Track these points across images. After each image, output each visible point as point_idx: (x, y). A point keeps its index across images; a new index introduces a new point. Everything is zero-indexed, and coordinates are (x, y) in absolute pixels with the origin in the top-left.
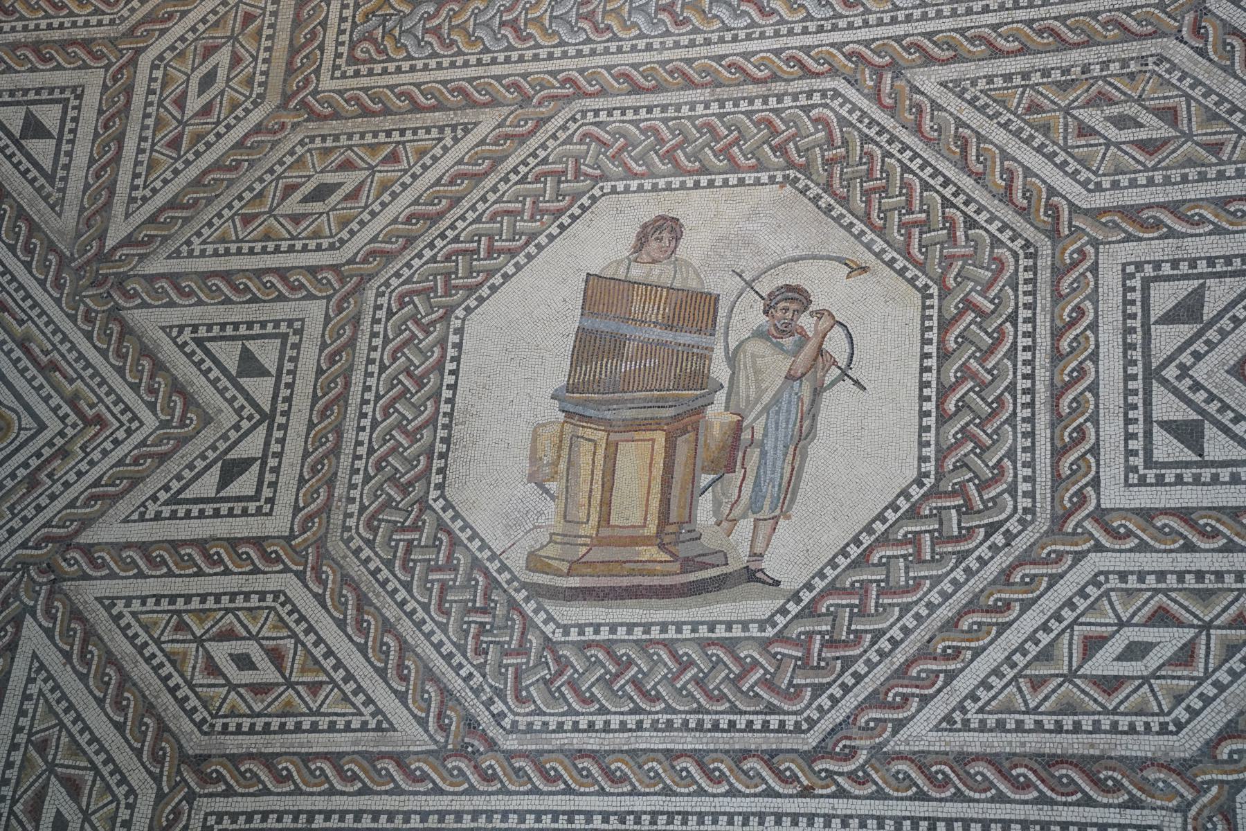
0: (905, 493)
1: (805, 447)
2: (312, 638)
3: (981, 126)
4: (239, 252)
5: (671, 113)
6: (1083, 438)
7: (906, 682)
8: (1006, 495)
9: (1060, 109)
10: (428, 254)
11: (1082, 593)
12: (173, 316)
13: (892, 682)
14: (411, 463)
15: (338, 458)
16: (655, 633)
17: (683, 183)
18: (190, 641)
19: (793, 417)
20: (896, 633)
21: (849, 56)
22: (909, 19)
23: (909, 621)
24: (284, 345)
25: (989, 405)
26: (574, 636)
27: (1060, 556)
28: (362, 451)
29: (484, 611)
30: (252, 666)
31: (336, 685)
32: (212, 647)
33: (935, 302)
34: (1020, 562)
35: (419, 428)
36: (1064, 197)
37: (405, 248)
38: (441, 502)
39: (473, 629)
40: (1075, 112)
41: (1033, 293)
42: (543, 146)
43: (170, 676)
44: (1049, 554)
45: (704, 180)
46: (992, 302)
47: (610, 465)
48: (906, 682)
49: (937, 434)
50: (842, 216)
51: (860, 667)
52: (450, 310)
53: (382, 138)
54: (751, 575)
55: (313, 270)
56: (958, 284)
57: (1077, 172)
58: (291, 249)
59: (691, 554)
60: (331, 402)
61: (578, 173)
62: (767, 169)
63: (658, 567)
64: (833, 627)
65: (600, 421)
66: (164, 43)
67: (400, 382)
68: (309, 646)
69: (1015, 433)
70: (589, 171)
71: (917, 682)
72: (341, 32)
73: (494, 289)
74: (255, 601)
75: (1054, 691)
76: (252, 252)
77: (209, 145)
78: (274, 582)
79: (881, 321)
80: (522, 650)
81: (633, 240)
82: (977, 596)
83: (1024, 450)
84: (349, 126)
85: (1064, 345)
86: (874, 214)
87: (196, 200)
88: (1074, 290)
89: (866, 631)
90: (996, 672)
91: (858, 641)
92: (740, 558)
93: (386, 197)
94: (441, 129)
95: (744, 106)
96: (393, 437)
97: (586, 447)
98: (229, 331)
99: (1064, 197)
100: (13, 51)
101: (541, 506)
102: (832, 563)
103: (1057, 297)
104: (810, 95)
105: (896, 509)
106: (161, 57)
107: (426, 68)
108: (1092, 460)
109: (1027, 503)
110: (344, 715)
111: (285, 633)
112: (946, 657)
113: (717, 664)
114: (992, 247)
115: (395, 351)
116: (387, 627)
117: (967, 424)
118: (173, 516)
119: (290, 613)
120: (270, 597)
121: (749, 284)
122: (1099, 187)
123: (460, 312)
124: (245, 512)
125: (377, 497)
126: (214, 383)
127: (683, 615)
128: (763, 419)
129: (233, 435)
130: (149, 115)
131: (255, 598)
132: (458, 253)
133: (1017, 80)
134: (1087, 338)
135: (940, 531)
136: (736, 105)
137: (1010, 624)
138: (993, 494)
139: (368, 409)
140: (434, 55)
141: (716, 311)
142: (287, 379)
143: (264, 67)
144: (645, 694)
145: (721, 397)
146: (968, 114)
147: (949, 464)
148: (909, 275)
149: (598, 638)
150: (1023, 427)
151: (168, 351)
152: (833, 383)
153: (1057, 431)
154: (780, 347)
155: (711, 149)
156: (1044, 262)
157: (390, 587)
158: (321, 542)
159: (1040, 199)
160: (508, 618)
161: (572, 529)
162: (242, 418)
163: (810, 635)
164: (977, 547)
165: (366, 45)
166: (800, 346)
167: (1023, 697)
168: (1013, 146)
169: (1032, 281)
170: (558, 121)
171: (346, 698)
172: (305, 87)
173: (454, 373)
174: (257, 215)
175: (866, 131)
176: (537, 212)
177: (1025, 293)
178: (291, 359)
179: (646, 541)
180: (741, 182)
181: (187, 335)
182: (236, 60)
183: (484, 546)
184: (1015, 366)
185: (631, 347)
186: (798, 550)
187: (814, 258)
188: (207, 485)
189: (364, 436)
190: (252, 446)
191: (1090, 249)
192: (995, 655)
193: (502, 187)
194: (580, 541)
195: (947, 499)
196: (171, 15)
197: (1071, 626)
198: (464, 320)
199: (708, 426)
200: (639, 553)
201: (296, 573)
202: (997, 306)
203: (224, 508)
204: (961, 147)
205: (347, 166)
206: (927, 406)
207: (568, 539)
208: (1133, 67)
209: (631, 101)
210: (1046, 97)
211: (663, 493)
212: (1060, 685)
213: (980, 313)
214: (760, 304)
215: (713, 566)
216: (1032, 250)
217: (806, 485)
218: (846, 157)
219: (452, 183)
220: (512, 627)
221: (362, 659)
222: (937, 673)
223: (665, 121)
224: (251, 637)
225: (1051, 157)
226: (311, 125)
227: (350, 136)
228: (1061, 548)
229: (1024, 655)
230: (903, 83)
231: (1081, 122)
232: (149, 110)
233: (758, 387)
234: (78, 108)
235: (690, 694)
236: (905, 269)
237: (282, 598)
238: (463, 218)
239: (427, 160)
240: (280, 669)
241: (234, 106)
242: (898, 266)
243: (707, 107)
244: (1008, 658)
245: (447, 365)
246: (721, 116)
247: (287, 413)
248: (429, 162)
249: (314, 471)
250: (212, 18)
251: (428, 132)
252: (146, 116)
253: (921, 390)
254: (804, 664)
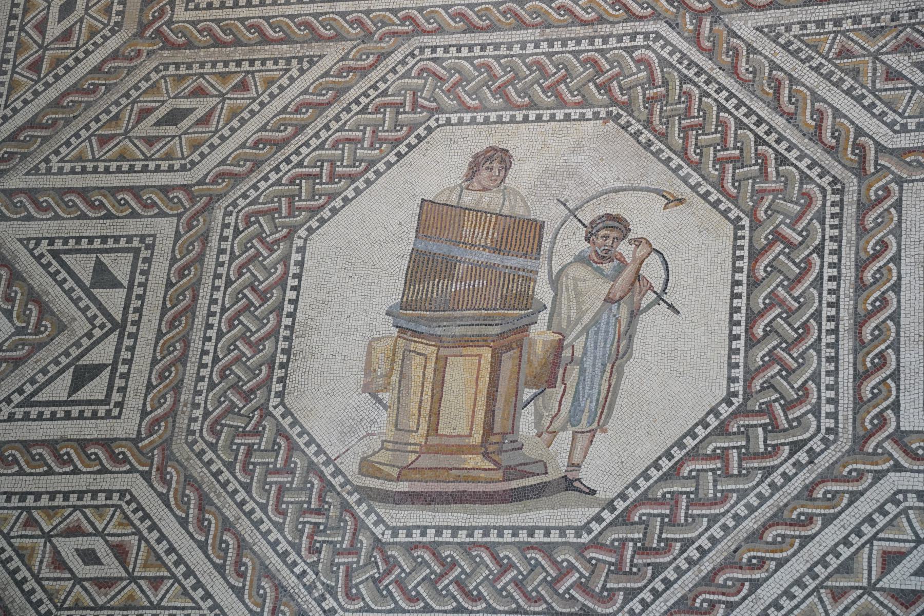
0: (714, 411)
1: (622, 366)
2: (155, 535)
3: (794, 69)
4: (95, 170)
5: (503, 51)
6: (884, 364)
7: (713, 589)
8: (810, 416)
9: (870, 54)
10: (273, 177)
11: (881, 510)
12: (31, 229)
13: (700, 589)
14: (253, 372)
15: (185, 366)
16: (478, 536)
17: (513, 117)
18: (38, 537)
19: (611, 337)
20: (704, 542)
23: (716, 531)
24: (136, 258)
25: (796, 330)
26: (402, 537)
27: (861, 474)
28: (207, 359)
29: (318, 512)
30: (97, 561)
31: (177, 580)
32: (59, 542)
33: (746, 233)
34: (822, 479)
35: (262, 340)
36: (871, 137)
37: (252, 171)
38: (281, 410)
39: (308, 529)
40: (883, 57)
41: (839, 227)
42: (384, 79)
43: (17, 570)
44: (850, 472)
45: (532, 115)
46: (800, 234)
47: (439, 378)
48: (713, 589)
49: (746, 357)
50: (661, 151)
51: (670, 574)
52: (293, 230)
53: (232, 67)
54: (569, 484)
55: (165, 190)
56: (769, 217)
57: (884, 114)
58: (145, 169)
59: (512, 463)
60: (179, 313)
61: (415, 105)
62: (591, 106)
63: (483, 474)
64: (645, 535)
65: (432, 336)
67: (245, 296)
68: (153, 542)
69: (819, 357)
70: (426, 103)
71: (723, 590)
73: (335, 212)
74: (101, 499)
75: (854, 602)
76: (107, 171)
77: (68, 69)
78: (120, 482)
79: (695, 249)
80: (353, 550)
81: (465, 169)
82: (781, 510)
83: (828, 373)
84: (202, 55)
85: (868, 276)
86: (691, 150)
87: (55, 121)
88: (879, 224)
89: (676, 540)
90: (799, 582)
91: (668, 549)
92: (558, 468)
93: (235, 123)
94: (288, 61)
95: (571, 46)
96: (237, 347)
97: (417, 361)
98: (84, 244)
99: (871, 137)
101: (373, 415)
102: (645, 475)
103: (862, 231)
104: (633, 37)
105: (706, 426)
108: (893, 385)
109: (831, 423)
110: (183, 609)
111: (129, 530)
112: (751, 567)
113: (535, 567)
114: (801, 183)
115: (241, 267)
116: (227, 525)
117: (774, 348)
118: (26, 417)
119: (135, 511)
120: (116, 496)
121: (573, 213)
122: (904, 129)
123: (302, 232)
124: (95, 416)
125: (220, 403)
126: (68, 292)
127: (505, 520)
128: (583, 339)
129: (86, 342)
130: (11, 39)
131: (102, 496)
132: (301, 176)
133: (830, 27)
134: (890, 270)
135: (747, 447)
136: (564, 45)
137: (812, 537)
138: (798, 414)
139: (214, 320)
141: (541, 237)
142: (138, 291)
144: (467, 594)
145: (544, 317)
146: (782, 58)
147: (757, 385)
148: (722, 207)
149: (425, 539)
150: (827, 352)
151: (25, 262)
152: (649, 307)
153: (860, 357)
154: (600, 271)
155: (540, 85)
156: (851, 197)
157: (230, 488)
158: (166, 445)
159: (847, 139)
160: (341, 519)
161: (403, 437)
162: (94, 327)
163: (623, 542)
164: (782, 464)
166: (619, 271)
167: (824, 607)
168: (824, 89)
169: (839, 216)
170: (398, 56)
171: (185, 593)
172: (160, 17)
173: (296, 288)
174: (112, 137)
175: (685, 71)
176: (376, 141)
177: (832, 227)
178: (143, 272)
179: (471, 449)
180: (567, 117)
181: (44, 247)
183: (320, 451)
184: (820, 294)
185: (461, 269)
186: (614, 461)
187: (634, 189)
188: (60, 389)
189: (209, 346)
190: (103, 353)
191: (894, 187)
192: (797, 566)
193: (344, 116)
194: (410, 448)
195: (755, 418)
197: (870, 541)
198: (306, 240)
199: (532, 344)
200: (465, 461)
201: (142, 474)
202: (805, 238)
203: (75, 411)
204: (774, 90)
205: (199, 92)
206: (737, 330)
207: (398, 447)
209: (466, 39)
210: (856, 43)
211: (488, 405)
212: (860, 597)
213: (789, 244)
214: (583, 232)
215: (534, 475)
216: (839, 186)
217: (621, 402)
218: (666, 96)
219: (297, 111)
220: (345, 528)
221: (202, 556)
222: (742, 582)
223: (497, 58)
224: (97, 533)
225: (859, 99)
226: (166, 53)
227: (202, 65)
228: (862, 467)
229: (826, 567)
230: (721, 27)
231: (889, 67)
232: (11, 34)
233: (579, 309)
235: (510, 595)
236: (718, 201)
237: (128, 497)
238: (307, 144)
239: (275, 89)
240: (123, 564)
241: (93, 33)
242: (712, 198)
243: (537, 46)
244: (810, 569)
245: (289, 280)
246: (549, 55)
247: (137, 323)
248: (276, 91)
249: (162, 377)
251: (276, 63)
253: (731, 315)
254: (617, 569)
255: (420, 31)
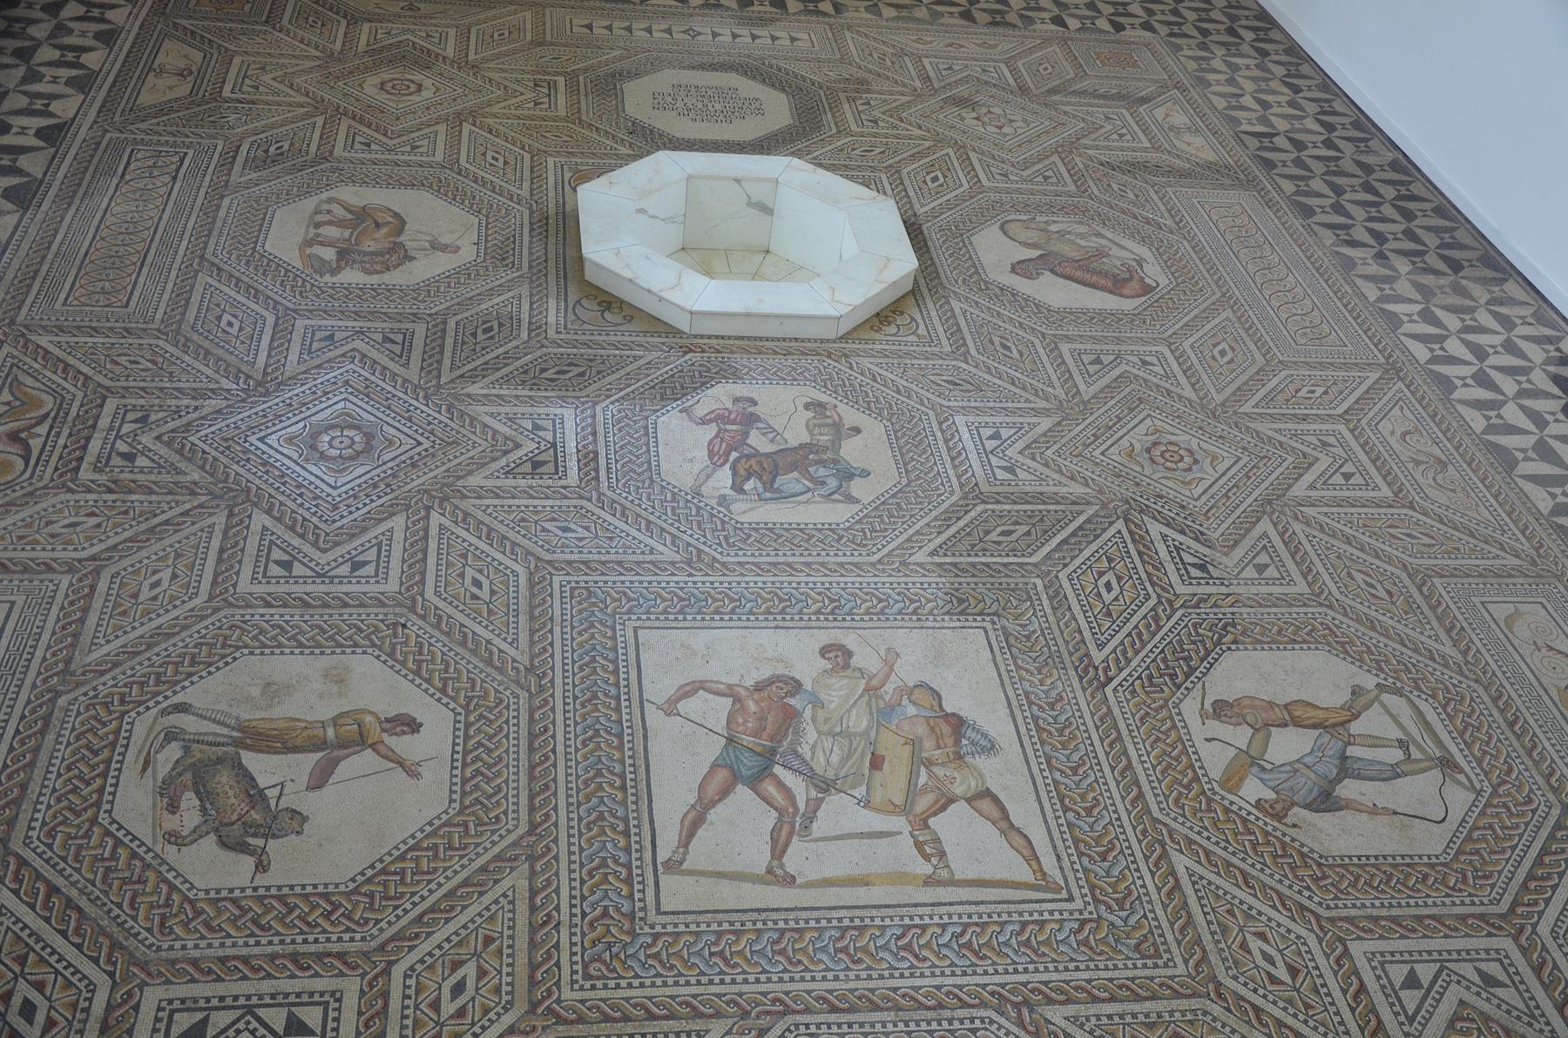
21: (992, 994)
22: (1026, 971)
66: (414, 957)
72: (573, 954)
100: (272, 961)
106: (412, 968)
107: (653, 985)
130: (407, 1017)
140: (658, 975)
143: (509, 979)
165: (597, 965)
172: (549, 996)
182: (482, 973)
196: (417, 936)
208: (1189, 1017)
209: (833, 1018)
226: (560, 1028)
232: (406, 1012)
234: (339, 1010)
241: (486, 1011)
243: (895, 1025)
250: (455, 939)
252: (404, 1017)
255: (788, 1011)
